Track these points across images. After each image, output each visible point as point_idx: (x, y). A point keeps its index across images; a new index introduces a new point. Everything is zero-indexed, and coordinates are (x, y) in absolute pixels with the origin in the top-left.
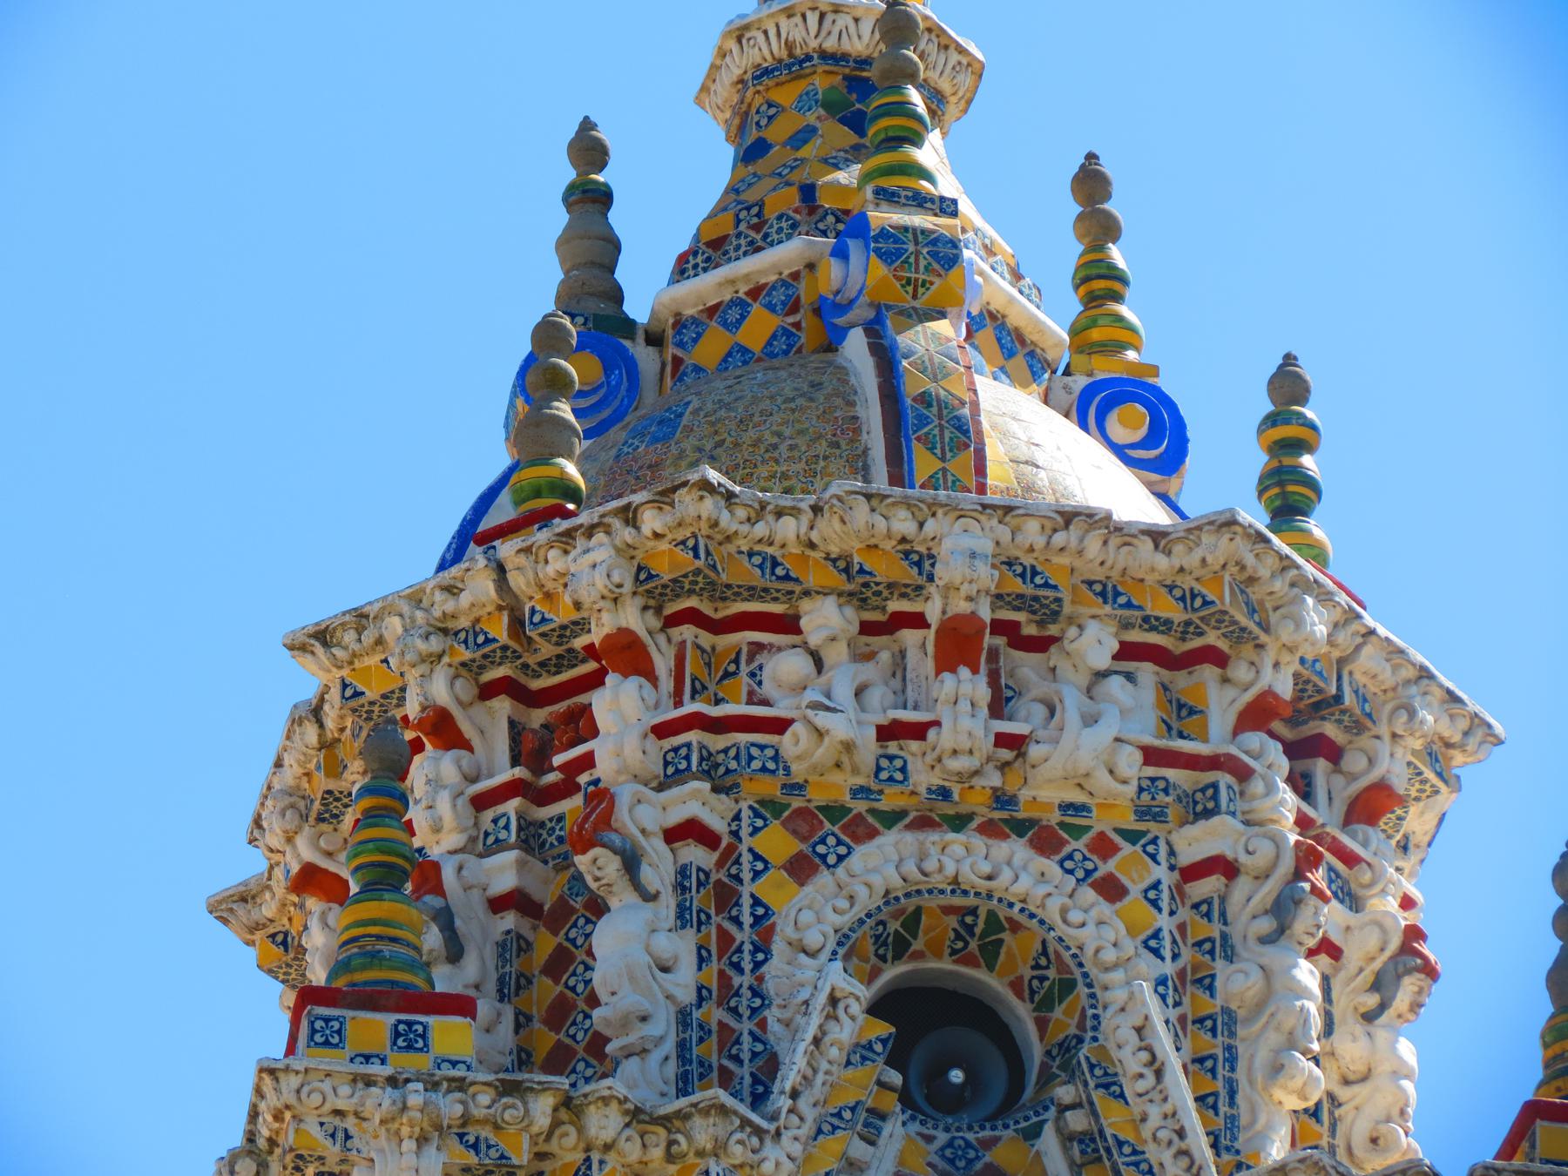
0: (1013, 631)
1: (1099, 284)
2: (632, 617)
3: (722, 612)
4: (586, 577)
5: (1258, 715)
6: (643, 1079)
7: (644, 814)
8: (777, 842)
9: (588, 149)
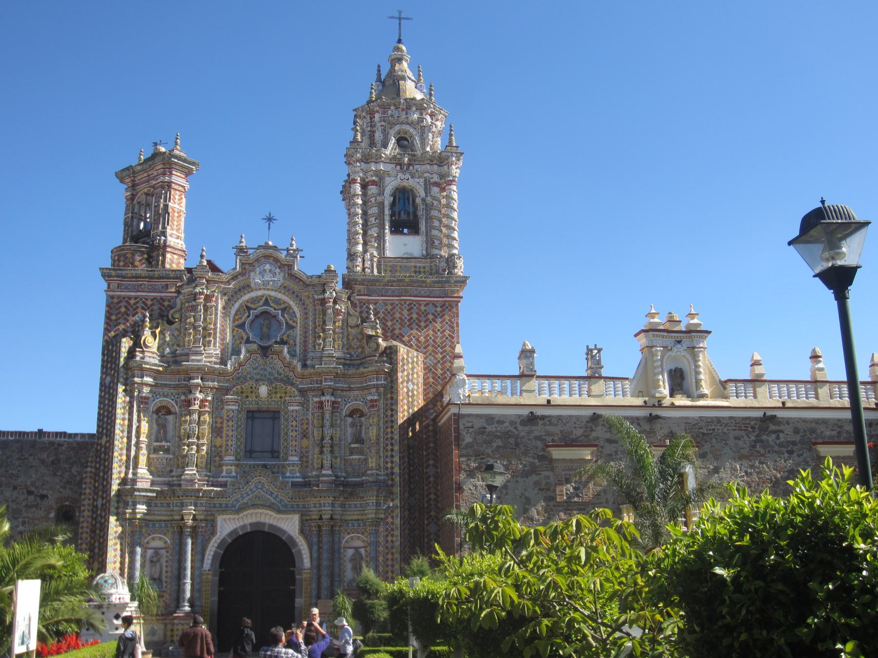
6: (379, 145)
8: (389, 126)
9: (379, 66)
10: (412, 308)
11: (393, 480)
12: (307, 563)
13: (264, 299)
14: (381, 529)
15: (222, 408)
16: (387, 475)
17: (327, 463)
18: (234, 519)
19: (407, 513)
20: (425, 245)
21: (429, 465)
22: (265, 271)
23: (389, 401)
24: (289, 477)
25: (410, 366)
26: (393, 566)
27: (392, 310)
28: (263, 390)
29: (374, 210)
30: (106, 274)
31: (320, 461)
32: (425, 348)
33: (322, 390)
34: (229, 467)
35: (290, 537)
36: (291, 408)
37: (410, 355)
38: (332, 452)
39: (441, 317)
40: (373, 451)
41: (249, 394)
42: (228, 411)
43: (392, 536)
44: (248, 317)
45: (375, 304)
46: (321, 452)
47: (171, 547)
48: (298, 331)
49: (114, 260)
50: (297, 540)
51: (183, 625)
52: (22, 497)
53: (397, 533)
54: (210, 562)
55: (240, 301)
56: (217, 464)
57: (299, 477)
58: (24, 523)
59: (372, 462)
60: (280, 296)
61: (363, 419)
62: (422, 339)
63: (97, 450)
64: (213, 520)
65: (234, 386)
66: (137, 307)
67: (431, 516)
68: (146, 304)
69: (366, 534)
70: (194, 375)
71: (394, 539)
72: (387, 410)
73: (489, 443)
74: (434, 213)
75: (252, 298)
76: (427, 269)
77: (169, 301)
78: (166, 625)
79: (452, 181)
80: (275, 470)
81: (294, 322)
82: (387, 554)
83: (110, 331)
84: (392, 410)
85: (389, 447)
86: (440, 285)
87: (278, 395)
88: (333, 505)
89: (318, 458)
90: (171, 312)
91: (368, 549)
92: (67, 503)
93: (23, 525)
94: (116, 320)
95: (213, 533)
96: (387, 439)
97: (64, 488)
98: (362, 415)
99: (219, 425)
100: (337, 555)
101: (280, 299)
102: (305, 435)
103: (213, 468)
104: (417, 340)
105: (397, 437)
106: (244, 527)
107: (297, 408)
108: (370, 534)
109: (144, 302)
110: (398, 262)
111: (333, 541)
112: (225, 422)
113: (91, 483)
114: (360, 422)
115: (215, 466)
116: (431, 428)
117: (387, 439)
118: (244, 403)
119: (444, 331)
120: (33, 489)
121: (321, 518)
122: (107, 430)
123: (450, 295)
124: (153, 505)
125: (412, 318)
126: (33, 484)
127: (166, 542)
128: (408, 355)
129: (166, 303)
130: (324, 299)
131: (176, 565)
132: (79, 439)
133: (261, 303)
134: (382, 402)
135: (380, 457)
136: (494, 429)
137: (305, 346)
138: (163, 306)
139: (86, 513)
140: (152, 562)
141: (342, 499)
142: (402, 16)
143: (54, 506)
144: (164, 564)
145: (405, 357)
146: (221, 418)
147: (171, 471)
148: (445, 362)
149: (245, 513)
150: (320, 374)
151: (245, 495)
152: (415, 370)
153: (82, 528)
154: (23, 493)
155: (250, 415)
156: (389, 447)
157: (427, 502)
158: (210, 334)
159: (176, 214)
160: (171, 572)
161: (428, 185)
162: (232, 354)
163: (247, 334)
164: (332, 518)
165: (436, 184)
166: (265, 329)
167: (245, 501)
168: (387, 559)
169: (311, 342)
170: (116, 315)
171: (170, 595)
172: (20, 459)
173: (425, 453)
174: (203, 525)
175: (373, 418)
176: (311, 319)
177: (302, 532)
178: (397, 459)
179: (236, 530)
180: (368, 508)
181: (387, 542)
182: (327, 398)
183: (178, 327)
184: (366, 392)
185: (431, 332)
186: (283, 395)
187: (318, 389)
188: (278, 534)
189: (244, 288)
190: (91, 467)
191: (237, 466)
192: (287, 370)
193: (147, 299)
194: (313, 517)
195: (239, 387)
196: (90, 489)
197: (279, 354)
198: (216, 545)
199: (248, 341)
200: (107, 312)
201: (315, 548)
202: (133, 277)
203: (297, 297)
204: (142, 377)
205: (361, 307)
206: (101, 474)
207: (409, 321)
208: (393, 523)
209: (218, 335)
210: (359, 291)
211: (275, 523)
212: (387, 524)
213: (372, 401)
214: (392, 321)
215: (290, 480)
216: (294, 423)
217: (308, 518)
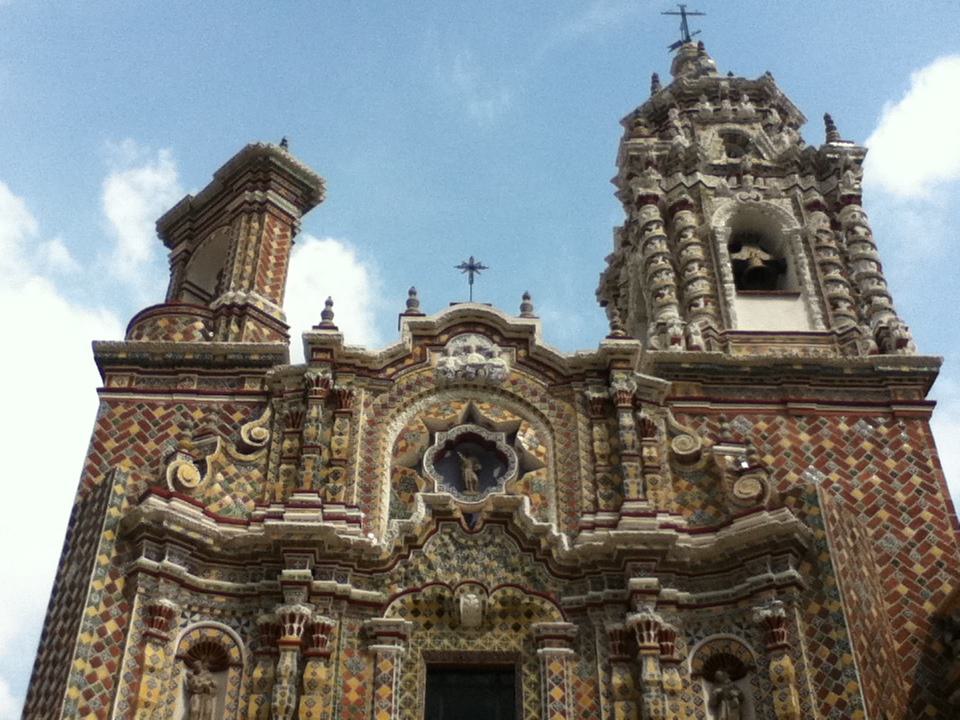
23: (819, 621)
27: (770, 431)
29: (697, 252)
62: (858, 494)
65: (395, 596)
66: (169, 425)
84: (830, 643)
94: (115, 451)
99: (353, 696)
109: (185, 415)
112: (370, 688)
119: (909, 476)
125: (821, 449)
138: (230, 421)
148: (928, 546)
170: (117, 441)
186: (524, 619)
193: (193, 409)
200: (97, 433)
204: (160, 558)
207: (816, 454)
209: (357, 478)
214: (774, 454)
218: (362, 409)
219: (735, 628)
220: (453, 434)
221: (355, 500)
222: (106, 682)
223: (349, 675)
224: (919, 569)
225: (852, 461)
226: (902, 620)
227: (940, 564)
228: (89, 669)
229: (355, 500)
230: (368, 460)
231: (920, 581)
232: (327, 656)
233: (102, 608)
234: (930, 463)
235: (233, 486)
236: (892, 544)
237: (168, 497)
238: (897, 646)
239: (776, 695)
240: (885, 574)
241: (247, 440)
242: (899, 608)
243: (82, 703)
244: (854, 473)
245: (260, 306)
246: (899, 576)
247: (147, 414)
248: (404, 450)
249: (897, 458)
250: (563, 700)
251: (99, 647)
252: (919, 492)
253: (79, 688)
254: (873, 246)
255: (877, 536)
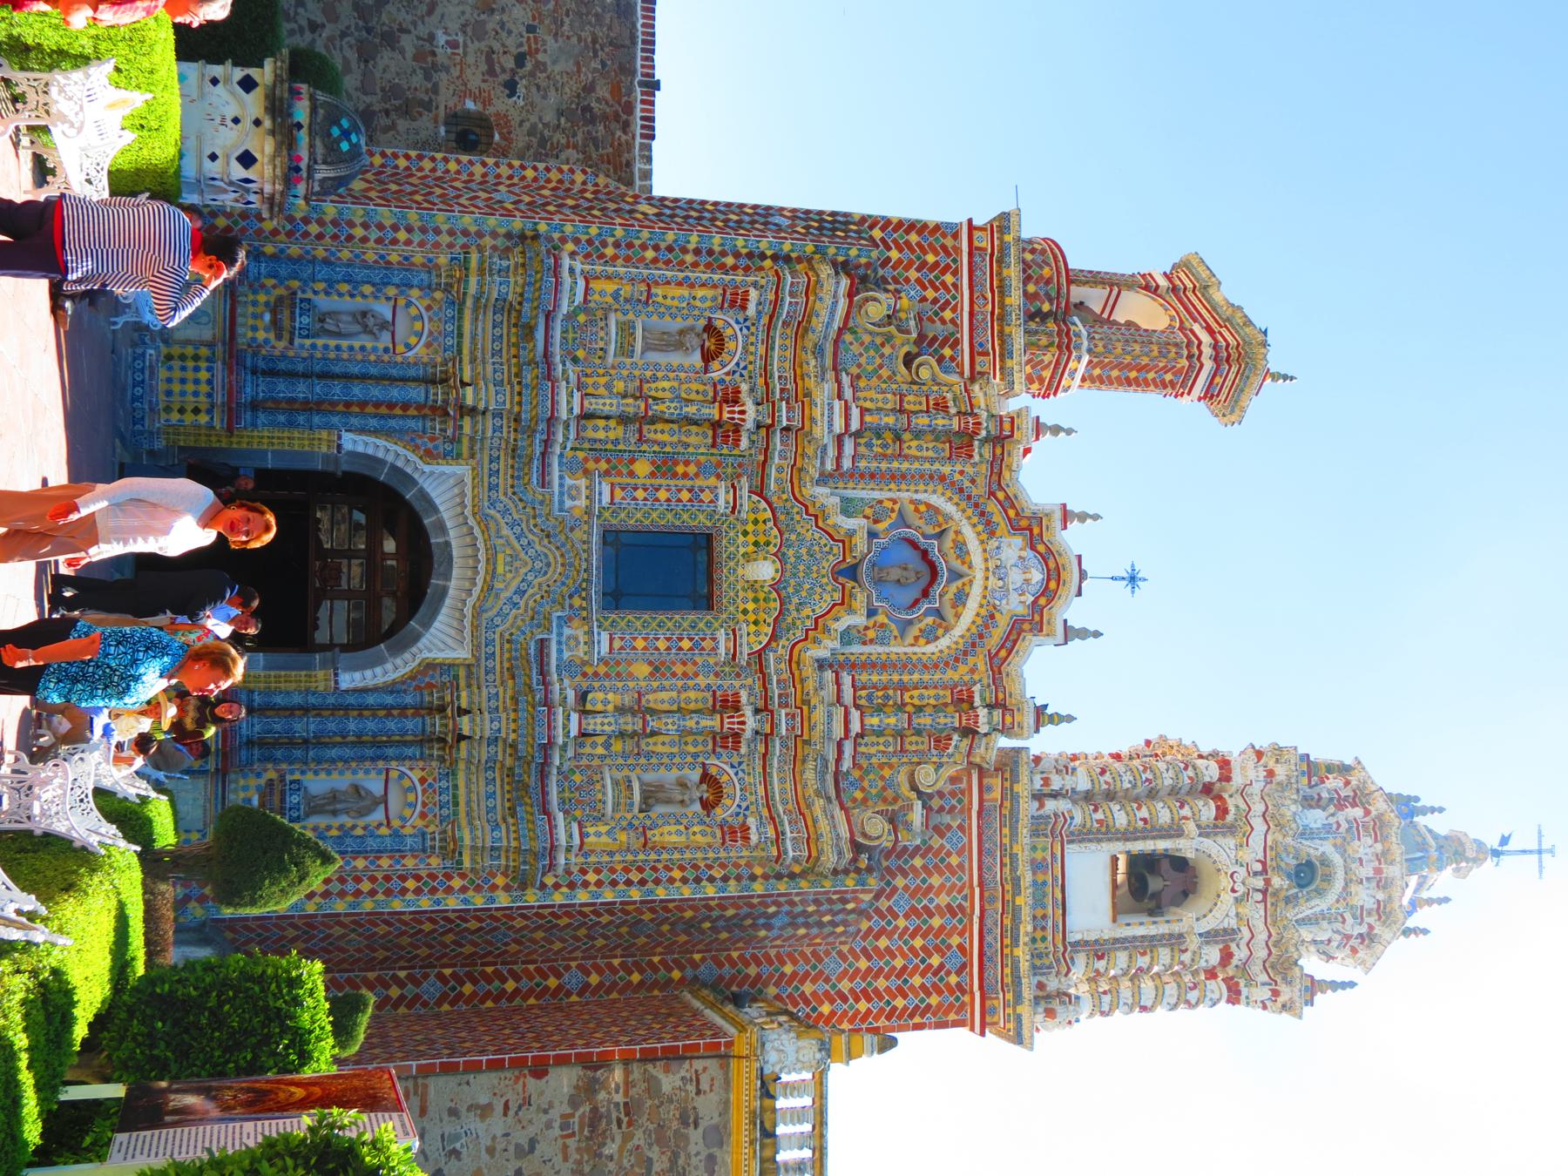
0: (1382, 883)
1: (1430, 902)
2: (1374, 813)
3: (1378, 828)
4: (1379, 806)
5: (1371, 927)
7: (1341, 817)
9: (1441, 810)
10: (954, 915)
11: (557, 886)
12: (349, 680)
13: (965, 568)
14: (435, 862)
15: (718, 476)
16: (568, 872)
17: (593, 724)
18: (462, 504)
19: (473, 925)
20: (1092, 937)
21: (588, 974)
22: (1026, 570)
23: (745, 872)
24: (560, 634)
25: (827, 919)
26: (342, 894)
28: (765, 571)
29: (1164, 817)
30: (1003, 223)
31: (599, 707)
32: (864, 951)
33: (766, 709)
34: (584, 492)
35: (417, 638)
36: (721, 635)
37: (851, 917)
38: (622, 735)
39: (934, 985)
40: (623, 837)
41: (751, 538)
42: (713, 489)
43: (418, 891)
44: (925, 536)
45: (961, 827)
46: (621, 710)
47: (399, 359)
48: (896, 649)
49: (1030, 242)
50: (407, 656)
51: (209, 382)
52: (511, 42)
53: (425, 904)
54: (360, 449)
55: (957, 515)
56: (591, 465)
57: (559, 659)
58: (453, 45)
59: (598, 834)
60: (973, 604)
61: (697, 807)
62: (883, 943)
63: (625, 195)
64: (459, 456)
66: (936, 289)
67: (462, 984)
68: (943, 309)
69: (420, 823)
70: (798, 411)
71: (410, 896)
72: (723, 866)
73: (660, 1136)
74: (1164, 954)
75: (965, 544)
76: (1040, 945)
77: (952, 359)
78: (211, 345)
79: (1238, 993)
80: (577, 602)
81: (916, 638)
82: (373, 879)
83: (883, 229)
85: (635, 876)
86: (1008, 980)
87: (751, 606)
88: (493, 741)
89: (606, 702)
90: (933, 362)
91: (384, 831)
92: (497, 137)
93: (447, 42)
94: (907, 243)
95: (429, 455)
96: (654, 869)
97: (531, 132)
98: (707, 806)
99: (680, 469)
100: (369, 752)
101: (964, 605)
102: (657, 670)
103: (581, 455)
104: (882, 932)
105: (661, 893)
106: (442, 528)
107: (722, 651)
108: (423, 834)
109: (947, 303)
110: (1054, 878)
111: (405, 743)
112: (689, 483)
113: (549, 181)
114: (692, 801)
115: (586, 460)
116: (676, 974)
117: (654, 869)
118: (731, 527)
119: (905, 996)
120: (529, 66)
121: (462, 712)
122: (672, 216)
123: (988, 1003)
124: (498, 317)
125: (931, 915)
126: (540, 67)
127: (409, 347)
128: (853, 911)
129: (947, 352)
130: (973, 708)
131: (356, 370)
132: (639, 165)
133: (956, 564)
134: (745, 853)
135: (611, 854)
136: (692, 1149)
137: (864, 666)
138: (942, 346)
139: (478, 170)
140: (364, 314)
141: (509, 762)
142: (1544, 856)
143: (491, 110)
144: (357, 344)
145: (850, 906)
146: (697, 475)
147: (575, 360)
148: (832, 1002)
149: (477, 532)
150: (808, 702)
151: (517, 529)
152: (815, 931)
153: (446, 160)
154: (521, 45)
155: (703, 542)
156: (635, 876)
157: (497, 973)
158: (885, 446)
159: (1133, 374)
160: (338, 359)
161: (1223, 937)
162: (846, 501)
163: (887, 530)
164: (461, 737)
165: (1227, 957)
166: (895, 574)
167: (506, 531)
168: (358, 880)
169: (875, 678)
170: (918, 244)
171: (284, 357)
172: (594, 41)
173: (616, 962)
174: (449, 432)
175: (704, 833)
176: (926, 677)
177: (430, 666)
178: (608, 896)
179: (435, 510)
180: (488, 828)
181: (403, 878)
182: (751, 722)
183: (898, 378)
184: (765, 813)
185: (899, 963)
186: (751, 617)
187: (766, 698)
188: (423, 610)
189: (988, 523)
190: (584, 183)
191: (588, 511)
192: (809, 623)
193: (954, 310)
194: (464, 694)
195: (769, 514)
196: (535, 180)
197: (845, 602)
198: (400, 464)
199: (872, 535)
200: (925, 226)
201: (389, 700)
202: (1001, 281)
203: (973, 644)
205: (953, 794)
206: (570, 202)
208: (449, 890)
209: (884, 466)
210: (990, 789)
211: (448, 601)
212: (449, 877)
213: (745, 829)
214: (924, 867)
215: (554, 637)
216: (686, 644)
217: (462, 683)
218: (958, 467)
219: (744, 805)
220: (935, 554)
221: (862, 464)
222: (682, 263)
223: (698, 464)
224: (808, 988)
225: (918, 942)
226: (758, 963)
227: (814, 1009)
228: (691, 247)
229: (862, 464)
230: (904, 477)
231: (797, 988)
232: (714, 445)
233: (744, 251)
234: (917, 1020)
235: (872, 352)
236: (832, 966)
237: (851, 295)
238: (735, 954)
239: (682, 828)
240: (803, 954)
241: (917, 361)
242: (771, 963)
243: (663, 245)
244: (905, 943)
245: (1071, 365)
246: (802, 968)
247: (947, 268)
248: (917, 510)
249: (923, 986)
250: (680, 649)
251: (710, 252)
252: (888, 1003)
253: (675, 241)
254: (1174, 1007)
255: (840, 953)
